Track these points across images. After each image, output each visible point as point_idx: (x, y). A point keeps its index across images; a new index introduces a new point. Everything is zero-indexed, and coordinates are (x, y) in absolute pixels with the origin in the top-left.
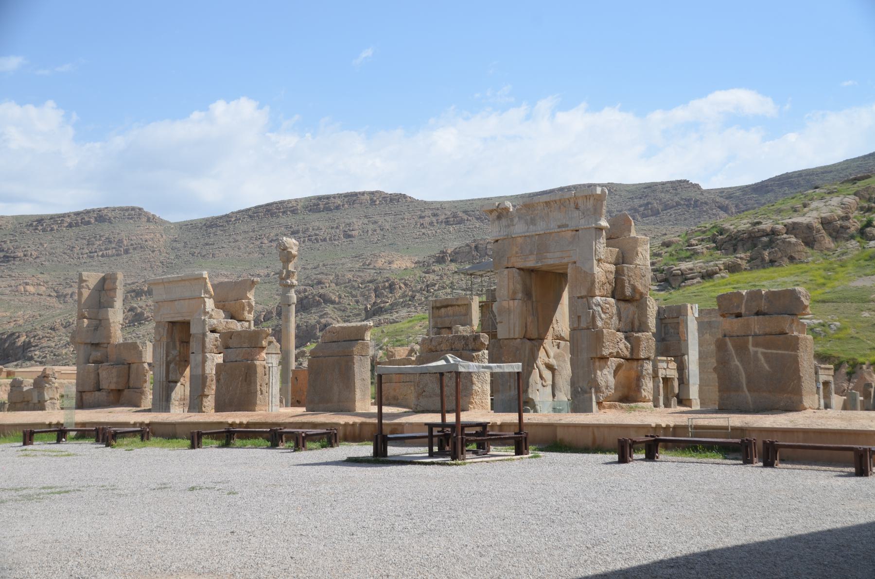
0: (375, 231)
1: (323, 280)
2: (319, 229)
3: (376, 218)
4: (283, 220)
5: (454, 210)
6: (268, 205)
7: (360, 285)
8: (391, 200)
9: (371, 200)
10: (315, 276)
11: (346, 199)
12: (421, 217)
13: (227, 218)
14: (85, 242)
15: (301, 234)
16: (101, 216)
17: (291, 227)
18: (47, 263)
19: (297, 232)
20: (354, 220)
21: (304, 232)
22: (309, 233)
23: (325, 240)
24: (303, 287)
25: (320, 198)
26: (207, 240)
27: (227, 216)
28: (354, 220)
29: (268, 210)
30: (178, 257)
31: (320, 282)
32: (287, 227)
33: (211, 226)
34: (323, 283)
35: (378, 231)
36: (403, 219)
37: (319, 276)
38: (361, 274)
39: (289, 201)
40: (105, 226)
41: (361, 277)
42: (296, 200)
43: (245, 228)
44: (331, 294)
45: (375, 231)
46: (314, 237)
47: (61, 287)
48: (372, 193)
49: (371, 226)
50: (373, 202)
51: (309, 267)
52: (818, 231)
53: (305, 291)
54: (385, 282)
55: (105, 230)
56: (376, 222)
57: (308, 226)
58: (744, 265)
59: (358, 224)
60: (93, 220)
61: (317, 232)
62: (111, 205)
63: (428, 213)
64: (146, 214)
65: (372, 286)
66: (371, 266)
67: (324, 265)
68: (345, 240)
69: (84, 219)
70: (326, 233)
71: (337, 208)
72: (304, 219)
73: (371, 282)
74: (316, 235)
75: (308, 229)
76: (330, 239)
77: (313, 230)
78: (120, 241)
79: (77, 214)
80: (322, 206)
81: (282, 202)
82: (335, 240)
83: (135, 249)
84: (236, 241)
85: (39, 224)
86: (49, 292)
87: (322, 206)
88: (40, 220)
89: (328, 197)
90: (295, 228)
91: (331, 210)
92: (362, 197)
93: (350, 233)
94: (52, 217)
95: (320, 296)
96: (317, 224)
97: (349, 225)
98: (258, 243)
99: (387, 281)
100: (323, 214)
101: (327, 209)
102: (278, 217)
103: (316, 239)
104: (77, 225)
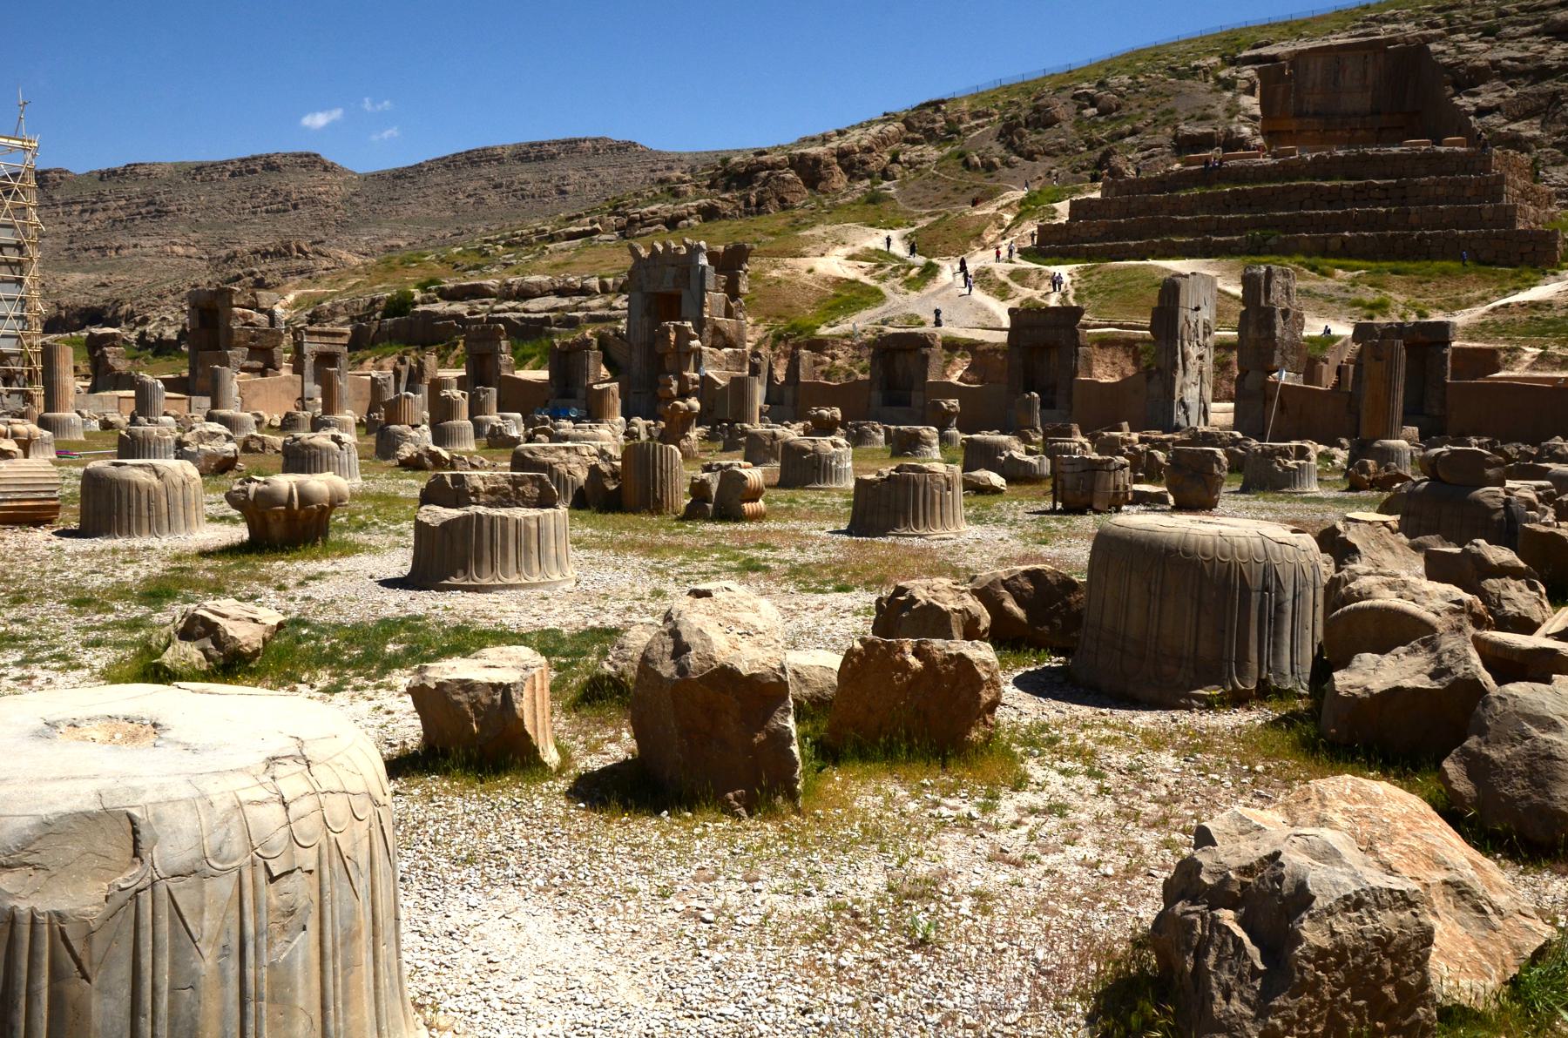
2: (527, 183)
5: (694, 163)
6: (468, 152)
12: (653, 171)
13: (418, 168)
15: (504, 189)
16: (268, 164)
18: (202, 220)
19: (500, 185)
20: (571, 172)
21: (508, 187)
25: (532, 145)
27: (420, 165)
29: (468, 159)
32: (489, 179)
33: (398, 177)
35: (599, 186)
36: (630, 172)
39: (493, 149)
43: (438, 180)
47: (214, 249)
49: (591, 180)
51: (493, 228)
52: (827, 166)
55: (273, 180)
58: (726, 208)
59: (574, 177)
60: (259, 169)
63: (661, 165)
64: (323, 162)
71: (552, 157)
74: (522, 189)
78: (289, 193)
79: (243, 160)
81: (484, 150)
83: (305, 204)
84: (426, 196)
85: (200, 172)
88: (200, 168)
89: (541, 144)
90: (498, 180)
91: (543, 160)
94: (213, 165)
97: (563, 178)
98: (452, 198)
100: (534, 165)
101: (539, 158)
104: (241, 173)
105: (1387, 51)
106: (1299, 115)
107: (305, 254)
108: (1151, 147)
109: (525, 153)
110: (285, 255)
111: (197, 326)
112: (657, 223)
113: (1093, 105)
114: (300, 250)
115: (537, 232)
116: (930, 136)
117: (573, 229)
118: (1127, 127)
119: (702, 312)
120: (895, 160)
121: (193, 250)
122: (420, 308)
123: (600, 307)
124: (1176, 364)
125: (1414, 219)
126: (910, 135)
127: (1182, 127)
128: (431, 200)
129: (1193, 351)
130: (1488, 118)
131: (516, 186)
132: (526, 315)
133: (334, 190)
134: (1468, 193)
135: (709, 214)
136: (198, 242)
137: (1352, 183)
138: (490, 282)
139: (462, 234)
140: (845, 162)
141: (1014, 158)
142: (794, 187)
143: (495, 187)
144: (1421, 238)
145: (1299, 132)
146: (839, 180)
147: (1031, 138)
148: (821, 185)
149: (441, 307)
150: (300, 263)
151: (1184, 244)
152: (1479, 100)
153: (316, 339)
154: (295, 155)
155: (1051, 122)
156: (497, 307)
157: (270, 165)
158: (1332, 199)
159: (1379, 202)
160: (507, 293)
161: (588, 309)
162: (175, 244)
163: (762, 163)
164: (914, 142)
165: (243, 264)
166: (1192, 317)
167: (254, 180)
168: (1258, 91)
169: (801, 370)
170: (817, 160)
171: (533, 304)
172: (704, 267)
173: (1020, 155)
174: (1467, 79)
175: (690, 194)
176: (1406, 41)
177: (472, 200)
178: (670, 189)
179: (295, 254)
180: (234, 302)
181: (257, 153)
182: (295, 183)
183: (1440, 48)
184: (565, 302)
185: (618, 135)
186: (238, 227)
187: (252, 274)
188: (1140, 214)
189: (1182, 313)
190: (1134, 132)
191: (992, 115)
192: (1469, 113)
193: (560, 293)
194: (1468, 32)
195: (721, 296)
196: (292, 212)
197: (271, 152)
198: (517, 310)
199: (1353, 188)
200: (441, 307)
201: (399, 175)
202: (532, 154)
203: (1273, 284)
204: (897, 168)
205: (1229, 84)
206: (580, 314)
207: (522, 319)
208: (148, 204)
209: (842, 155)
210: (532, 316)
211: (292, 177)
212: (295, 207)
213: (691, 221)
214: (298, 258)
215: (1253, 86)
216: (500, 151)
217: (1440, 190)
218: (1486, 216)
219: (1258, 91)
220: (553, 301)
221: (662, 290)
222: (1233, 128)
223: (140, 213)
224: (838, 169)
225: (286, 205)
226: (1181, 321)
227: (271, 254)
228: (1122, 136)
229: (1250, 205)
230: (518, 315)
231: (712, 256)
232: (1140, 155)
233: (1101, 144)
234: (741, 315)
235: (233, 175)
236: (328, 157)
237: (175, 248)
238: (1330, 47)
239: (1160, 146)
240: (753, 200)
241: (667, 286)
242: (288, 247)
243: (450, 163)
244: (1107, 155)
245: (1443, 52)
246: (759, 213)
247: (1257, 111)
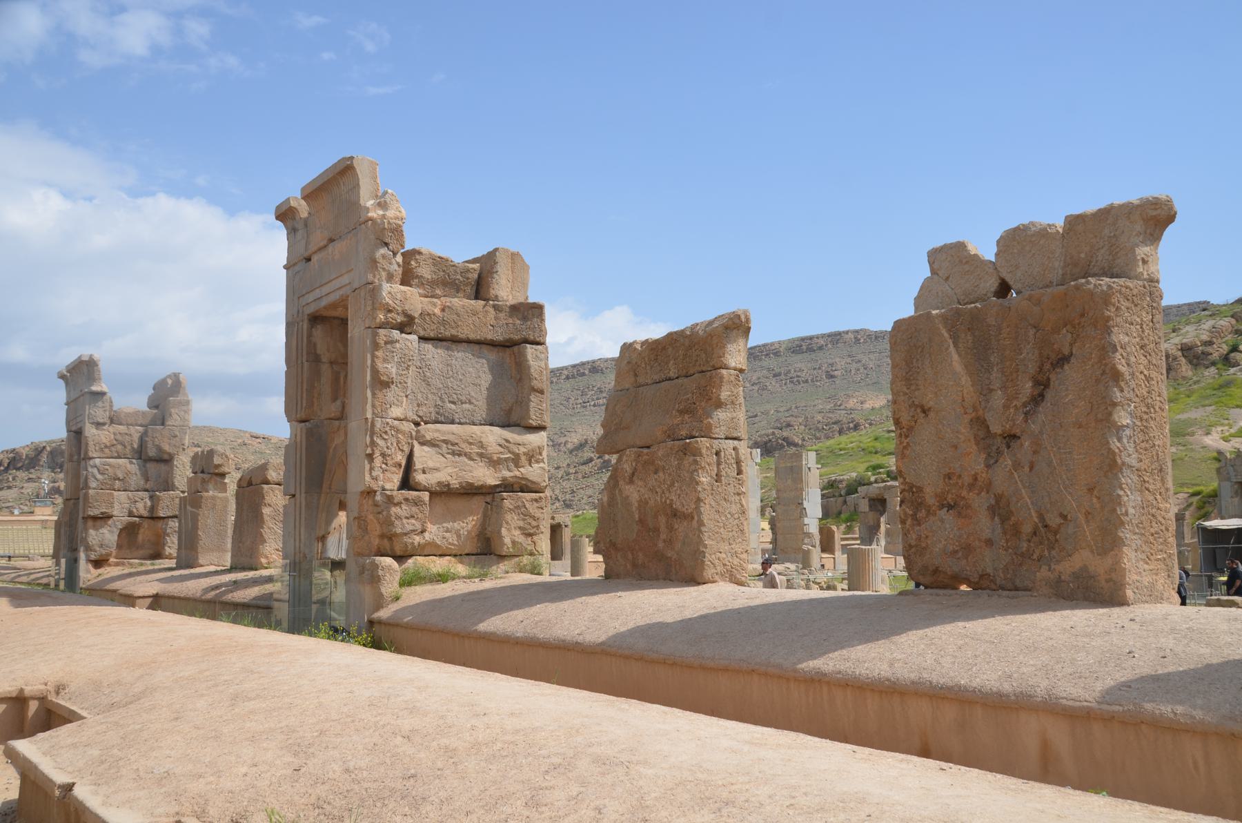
0: (858, 370)
1: (792, 423)
3: (860, 357)
4: (766, 362)
7: (825, 427)
9: (855, 338)
10: (784, 419)
11: (830, 339)
14: (579, 392)
15: (783, 377)
17: (773, 370)
19: (779, 374)
20: (837, 360)
21: (785, 375)
22: (790, 375)
23: (807, 381)
24: (772, 430)
25: (803, 339)
28: (837, 360)
31: (789, 425)
32: (769, 369)
34: (792, 426)
37: (788, 419)
38: (831, 415)
39: (772, 344)
41: (830, 418)
42: (779, 343)
44: (795, 437)
45: (858, 370)
46: (795, 379)
48: (857, 331)
49: (855, 365)
50: (857, 340)
51: (782, 410)
53: (773, 432)
54: (849, 423)
56: (860, 361)
57: (790, 368)
59: (841, 363)
61: (799, 374)
65: (836, 427)
66: (842, 407)
67: (796, 407)
68: (827, 381)
69: (579, 371)
70: (808, 375)
71: (821, 348)
72: (786, 360)
73: (835, 423)
74: (798, 376)
75: (790, 370)
76: (812, 381)
77: (795, 371)
80: (804, 347)
81: (764, 345)
82: (817, 381)
87: (804, 347)
89: (811, 338)
90: (777, 370)
92: (846, 336)
93: (832, 373)
95: (784, 440)
96: (799, 365)
97: (832, 365)
99: (852, 422)
101: (810, 350)
102: (761, 360)
103: (798, 381)
109: (797, 346)
131: (793, 374)
139: (756, 416)
143: (775, 376)
177: (756, 388)
186: (574, 419)
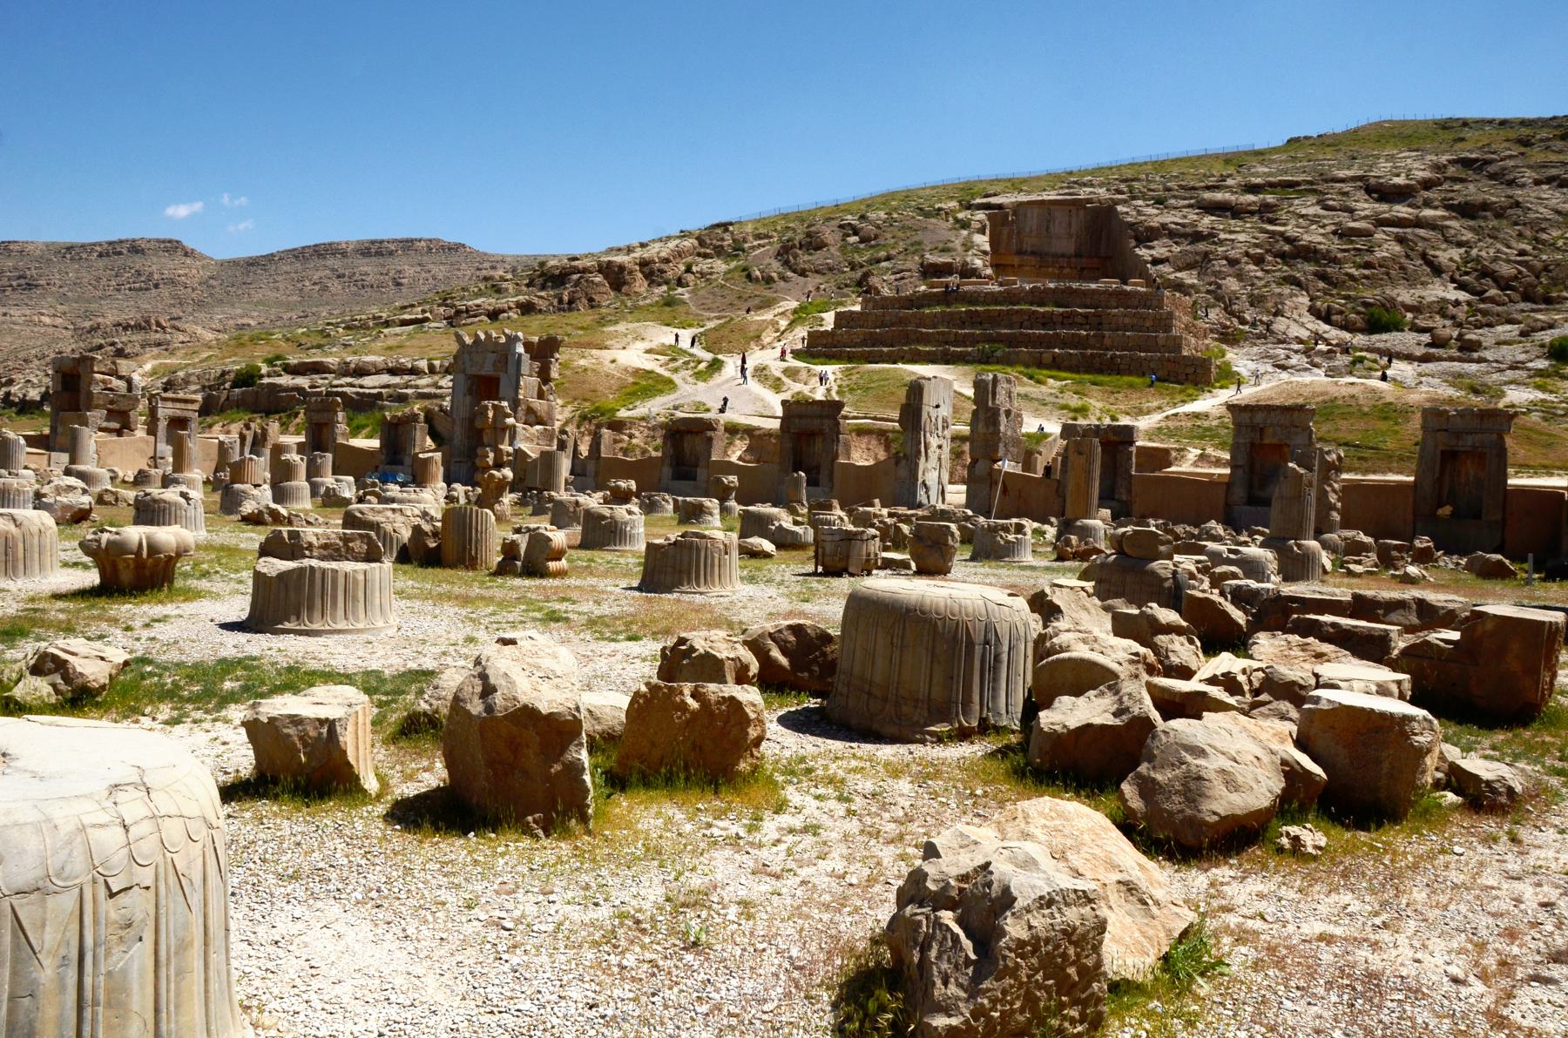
2: (367, 274)
4: (330, 262)
5: (515, 264)
6: (316, 246)
8: (450, 249)
15: (346, 279)
18: (69, 294)
19: (344, 276)
20: (406, 267)
25: (373, 242)
26: (245, 279)
27: (272, 255)
28: (406, 267)
30: (211, 295)
32: (333, 270)
33: (252, 264)
35: (431, 280)
39: (338, 244)
40: (137, 258)
49: (424, 275)
52: (631, 272)
55: (138, 262)
58: (542, 304)
59: (410, 271)
60: (125, 251)
62: (148, 236)
64: (184, 248)
71: (391, 253)
78: (151, 274)
79: (110, 243)
81: (330, 244)
84: (275, 282)
85: (71, 252)
86: (66, 324)
88: (70, 248)
89: (381, 242)
90: (341, 271)
94: (83, 246)
96: (366, 269)
97: (400, 272)
98: (300, 285)
100: (374, 259)
101: (379, 254)
104: (108, 255)
105: (1085, 208)
106: (1020, 252)
107: (163, 328)
108: (902, 271)
110: (144, 328)
111: (60, 389)
112: (481, 314)
113: (856, 233)
114: (158, 324)
115: (374, 318)
116: (719, 252)
117: (407, 317)
118: (883, 254)
119: (517, 393)
120: (688, 270)
121: (59, 321)
122: (266, 381)
123: (428, 386)
124: (920, 452)
125: (1107, 342)
126: (702, 250)
127: (928, 256)
128: (281, 286)
129: (934, 442)
130: (1160, 267)
132: (361, 390)
133: (192, 273)
134: (1148, 324)
135: (527, 309)
136: (65, 313)
137: (1061, 310)
138: (330, 360)
140: (646, 270)
141: (789, 274)
142: (603, 289)
143: (339, 277)
144: (1112, 358)
145: (1020, 266)
146: (640, 284)
147: (804, 259)
148: (624, 289)
149: (285, 380)
150: (158, 336)
151: (928, 352)
152: (1153, 252)
153: (170, 404)
154: (158, 241)
155: (820, 246)
156: (336, 382)
157: (135, 248)
158: (1047, 321)
159: (1081, 326)
160: (345, 370)
161: (417, 387)
162: (43, 314)
163: (574, 267)
164: (706, 256)
165: (105, 335)
166: (933, 413)
167: (120, 261)
168: (988, 232)
169: (602, 448)
170: (622, 268)
171: (368, 381)
172: (520, 355)
173: (794, 271)
174: (1147, 236)
175: (511, 291)
176: (1100, 201)
177: (317, 287)
178: (493, 286)
179: (154, 328)
180: (96, 369)
181: (123, 237)
182: (156, 265)
183: (1125, 209)
184: (396, 380)
185: (450, 237)
187: (113, 344)
188: (892, 325)
189: (926, 409)
190: (888, 258)
191: (771, 237)
192: (1147, 262)
193: (393, 372)
194: (1145, 200)
195: (535, 380)
196: (154, 291)
197: (137, 236)
198: (353, 386)
199: (1062, 314)
200: (285, 380)
201: (252, 263)
202: (373, 250)
203: (999, 389)
204: (690, 277)
205: (965, 225)
206: (409, 391)
207: (357, 393)
208: (20, 277)
209: (644, 264)
210: (367, 391)
211: (155, 259)
212: (156, 286)
213: (511, 314)
214: (156, 331)
215: (984, 227)
216: (344, 246)
217: (1127, 320)
218: (1161, 342)
219: (988, 232)
220: (386, 379)
221: (483, 373)
222: (968, 259)
223: (11, 286)
224: (640, 275)
225: (150, 284)
226: (924, 416)
227: (132, 327)
228: (879, 261)
229: (981, 323)
230: (354, 390)
231: (528, 346)
232: (893, 277)
233: (862, 266)
234: (551, 398)
235: (100, 255)
236: (189, 243)
237: (42, 318)
238: (1043, 202)
239: (910, 271)
240: (566, 298)
241: (487, 370)
242: (148, 322)
243: (299, 255)
244: (866, 275)
245: (1127, 213)
246: (570, 310)
247: (987, 247)
